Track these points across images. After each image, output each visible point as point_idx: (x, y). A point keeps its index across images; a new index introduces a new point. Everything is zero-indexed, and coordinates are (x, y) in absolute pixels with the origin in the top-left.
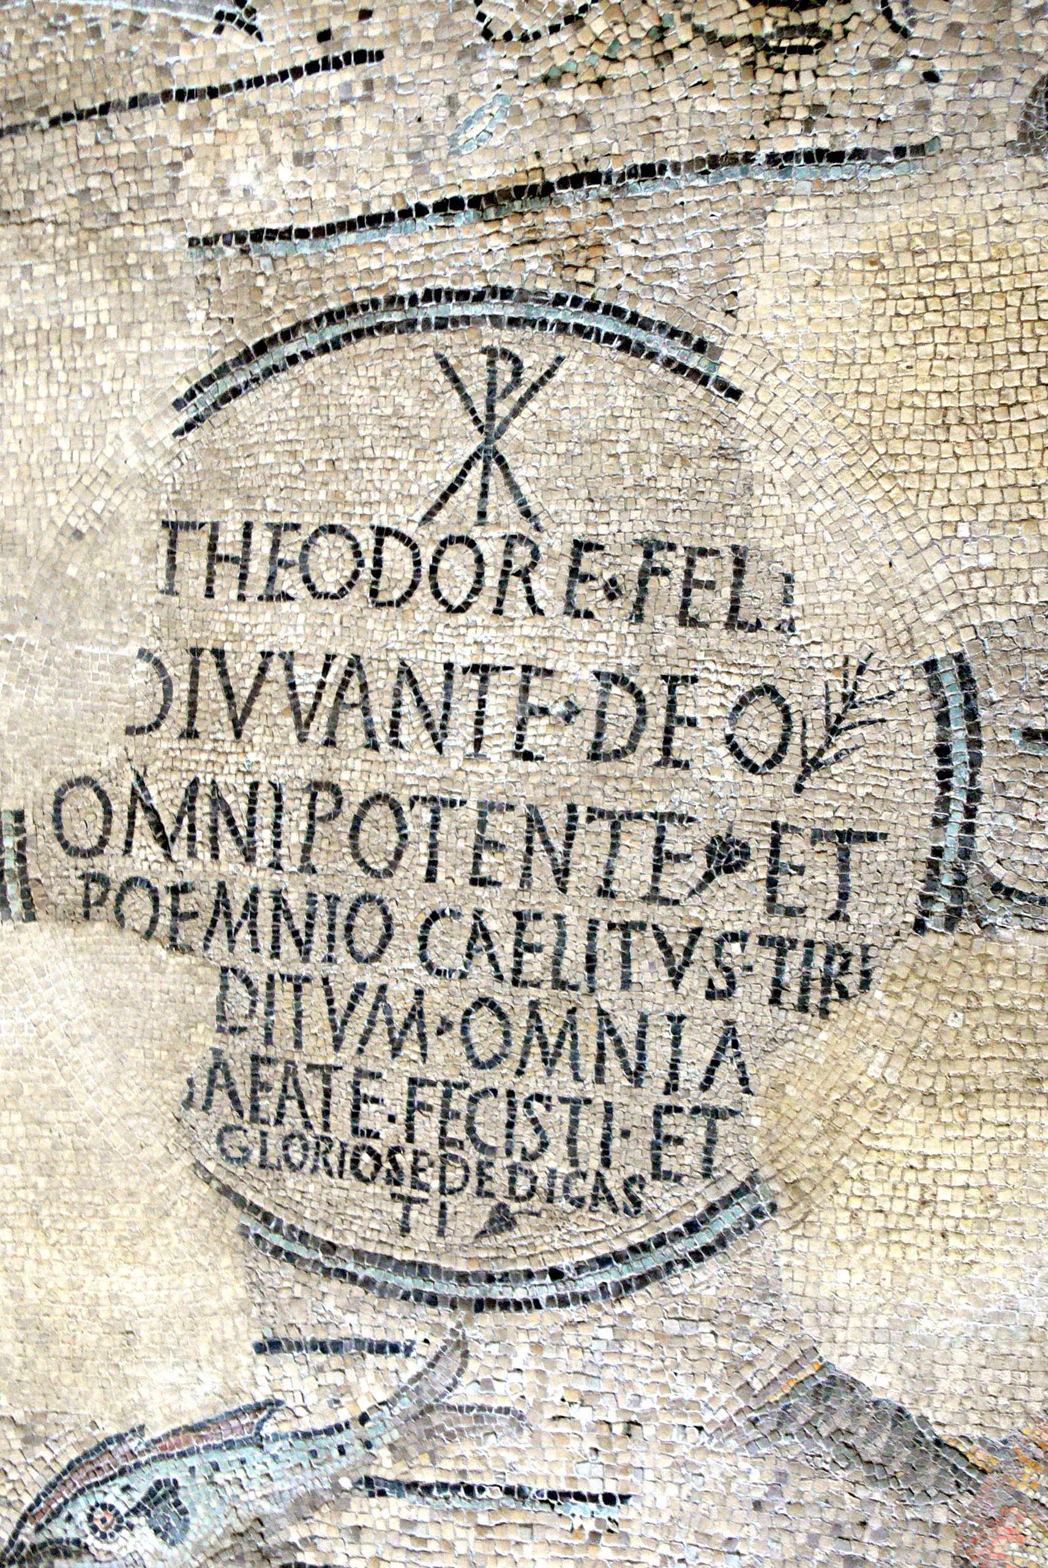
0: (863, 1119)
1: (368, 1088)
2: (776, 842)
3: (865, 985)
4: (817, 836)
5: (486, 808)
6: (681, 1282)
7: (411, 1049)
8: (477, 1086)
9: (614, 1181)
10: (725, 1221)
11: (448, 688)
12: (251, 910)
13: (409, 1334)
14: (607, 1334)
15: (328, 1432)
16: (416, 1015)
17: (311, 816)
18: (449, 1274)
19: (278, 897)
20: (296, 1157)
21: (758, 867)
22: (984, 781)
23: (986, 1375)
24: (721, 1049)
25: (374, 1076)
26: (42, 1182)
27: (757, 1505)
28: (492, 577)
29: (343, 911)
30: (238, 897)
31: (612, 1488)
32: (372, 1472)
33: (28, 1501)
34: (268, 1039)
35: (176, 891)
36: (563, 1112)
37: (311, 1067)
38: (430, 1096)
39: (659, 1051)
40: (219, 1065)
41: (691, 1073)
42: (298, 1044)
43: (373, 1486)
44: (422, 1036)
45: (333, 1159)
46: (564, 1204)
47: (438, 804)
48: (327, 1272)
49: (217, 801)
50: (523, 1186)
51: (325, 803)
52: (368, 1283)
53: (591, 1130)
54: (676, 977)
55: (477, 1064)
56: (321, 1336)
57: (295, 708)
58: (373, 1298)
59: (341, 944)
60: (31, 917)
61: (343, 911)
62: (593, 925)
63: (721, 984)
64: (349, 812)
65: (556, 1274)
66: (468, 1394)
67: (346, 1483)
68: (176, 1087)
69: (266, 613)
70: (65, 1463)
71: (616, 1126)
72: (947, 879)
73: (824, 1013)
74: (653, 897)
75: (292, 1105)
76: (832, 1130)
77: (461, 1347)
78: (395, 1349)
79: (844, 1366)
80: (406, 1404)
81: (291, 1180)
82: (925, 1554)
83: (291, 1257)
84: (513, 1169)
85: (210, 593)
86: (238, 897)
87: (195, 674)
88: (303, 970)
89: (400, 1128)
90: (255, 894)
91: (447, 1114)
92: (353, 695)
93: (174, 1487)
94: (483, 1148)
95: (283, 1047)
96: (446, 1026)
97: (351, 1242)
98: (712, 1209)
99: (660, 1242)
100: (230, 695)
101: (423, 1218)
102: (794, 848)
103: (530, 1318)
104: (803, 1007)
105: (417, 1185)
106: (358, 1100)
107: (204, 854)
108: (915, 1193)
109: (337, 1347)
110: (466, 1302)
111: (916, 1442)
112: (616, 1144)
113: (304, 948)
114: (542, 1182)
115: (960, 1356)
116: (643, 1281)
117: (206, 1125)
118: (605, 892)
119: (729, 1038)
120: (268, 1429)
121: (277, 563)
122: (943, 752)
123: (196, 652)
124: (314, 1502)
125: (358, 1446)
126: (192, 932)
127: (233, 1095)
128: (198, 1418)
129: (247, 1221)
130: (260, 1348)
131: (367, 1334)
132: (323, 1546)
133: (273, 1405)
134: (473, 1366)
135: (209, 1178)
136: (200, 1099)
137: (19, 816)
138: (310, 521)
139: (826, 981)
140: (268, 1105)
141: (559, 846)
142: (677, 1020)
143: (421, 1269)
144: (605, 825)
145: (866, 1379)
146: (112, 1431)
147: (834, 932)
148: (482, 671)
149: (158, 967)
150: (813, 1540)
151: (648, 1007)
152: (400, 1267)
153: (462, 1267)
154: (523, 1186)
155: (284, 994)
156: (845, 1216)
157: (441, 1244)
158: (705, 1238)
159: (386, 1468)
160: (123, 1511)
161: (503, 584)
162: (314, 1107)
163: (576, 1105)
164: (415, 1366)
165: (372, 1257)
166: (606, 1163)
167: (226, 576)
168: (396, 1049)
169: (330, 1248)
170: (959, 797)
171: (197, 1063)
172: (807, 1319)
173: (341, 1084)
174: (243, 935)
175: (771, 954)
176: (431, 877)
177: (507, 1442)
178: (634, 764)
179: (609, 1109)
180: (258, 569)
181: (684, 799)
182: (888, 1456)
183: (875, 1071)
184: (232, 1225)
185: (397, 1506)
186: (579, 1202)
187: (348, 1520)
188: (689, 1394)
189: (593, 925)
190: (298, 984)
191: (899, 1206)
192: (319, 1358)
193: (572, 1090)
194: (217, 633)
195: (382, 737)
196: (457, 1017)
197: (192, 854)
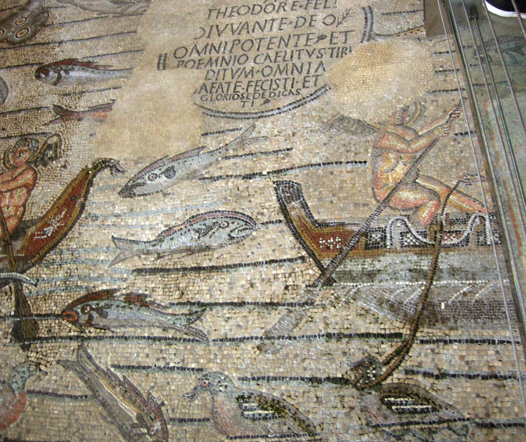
0: (350, 72)
1: (238, 84)
2: (332, 35)
3: (350, 51)
4: (340, 33)
5: (271, 39)
6: (308, 106)
7: (250, 76)
8: (263, 80)
9: (294, 90)
10: (319, 93)
11: (266, 23)
12: (217, 61)
13: (241, 126)
14: (290, 116)
15: (217, 150)
16: (252, 71)
17: (233, 45)
18: (253, 113)
19: (223, 58)
20: (219, 98)
21: (329, 38)
22: (374, 21)
23: (379, 111)
24: (319, 65)
25: (241, 82)
26: (154, 113)
27: (325, 144)
28: (276, 8)
29: (237, 58)
30: (214, 59)
31: (288, 147)
32: (228, 155)
33: (132, 176)
34: (217, 79)
35: (200, 60)
36: (283, 81)
37: (226, 83)
38: (254, 84)
39: (306, 68)
40: (204, 85)
41: (312, 71)
42: (223, 79)
43: (227, 158)
44: (253, 75)
45: (228, 97)
46: (282, 97)
47: (260, 40)
48: (223, 117)
49: (212, 45)
50: (272, 95)
51: (237, 42)
52: (233, 118)
53: (289, 83)
54: (310, 56)
55: (264, 76)
56: (219, 130)
57: (232, 30)
58: (233, 120)
59: (236, 62)
60: (164, 68)
61: (237, 58)
62: (292, 52)
63: (319, 56)
64: (241, 43)
65: (279, 109)
66: (254, 135)
67: (220, 159)
68: (192, 91)
69: (229, 19)
70: (144, 167)
71: (295, 81)
72: (367, 35)
73: (342, 57)
74: (306, 45)
75: (220, 90)
76: (343, 74)
77: (254, 126)
78: (237, 129)
79: (346, 115)
80: (238, 140)
81: (217, 103)
82: (366, 147)
83: (214, 116)
84: (271, 93)
85: (217, 18)
86: (214, 59)
87: (211, 29)
88: (227, 67)
89: (245, 90)
90: (218, 58)
91: (256, 85)
92: (246, 26)
93: (173, 167)
94: (264, 90)
95: (220, 80)
96: (258, 71)
97: (230, 110)
98: (316, 91)
99: (304, 98)
100: (218, 31)
101: (248, 104)
102: (335, 35)
103: (272, 118)
104: (337, 57)
105: (247, 98)
106: (236, 86)
107: (208, 53)
108: (362, 82)
109: (223, 132)
110: (256, 118)
111: (363, 126)
112: (295, 83)
113: (227, 64)
114: (277, 94)
115: (373, 108)
116: (299, 106)
117: (197, 97)
118: (296, 46)
119: (321, 63)
120: (201, 153)
121: (232, 11)
122: (366, 18)
123: (212, 26)
124: (211, 164)
125: (225, 151)
126: (203, 66)
127: (206, 91)
128: (183, 152)
129: (205, 111)
130: (203, 135)
131: (231, 128)
132: (211, 173)
133: (203, 147)
134: (256, 129)
135: (196, 104)
136: (199, 90)
137: (166, 54)
138: (240, 5)
139: (342, 53)
140: (214, 90)
141: (286, 41)
142: (310, 64)
143: (246, 114)
144: (297, 37)
145: (351, 116)
146: (160, 158)
147: (344, 45)
148: (273, 20)
149: (193, 72)
150: (338, 148)
151: (304, 61)
152: (241, 114)
153: (256, 111)
154: (272, 95)
155: (222, 73)
156: (346, 88)
157: (251, 108)
158: (314, 96)
159: (231, 152)
160: (158, 174)
161: (279, 9)
162: (225, 90)
163: (286, 79)
164: (241, 132)
165: (234, 113)
166: (292, 87)
167: (221, 16)
168: (246, 76)
169: (224, 113)
170: (369, 24)
171: (198, 86)
172: (337, 107)
173: (232, 86)
174: (215, 64)
175: (330, 51)
176: (258, 50)
177: (262, 143)
178: (303, 27)
179: (294, 78)
180: (228, 14)
181: (313, 31)
182: (357, 129)
183: (353, 64)
184: (201, 112)
185: (232, 161)
186: (286, 95)
187: (219, 166)
188: (309, 125)
189: (292, 52)
190: (225, 70)
191: (358, 84)
192: (218, 134)
193: (285, 77)
194: (217, 22)
195: (250, 32)
196: (261, 70)
197: (205, 54)
